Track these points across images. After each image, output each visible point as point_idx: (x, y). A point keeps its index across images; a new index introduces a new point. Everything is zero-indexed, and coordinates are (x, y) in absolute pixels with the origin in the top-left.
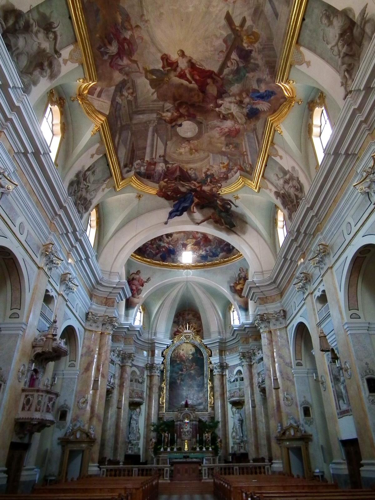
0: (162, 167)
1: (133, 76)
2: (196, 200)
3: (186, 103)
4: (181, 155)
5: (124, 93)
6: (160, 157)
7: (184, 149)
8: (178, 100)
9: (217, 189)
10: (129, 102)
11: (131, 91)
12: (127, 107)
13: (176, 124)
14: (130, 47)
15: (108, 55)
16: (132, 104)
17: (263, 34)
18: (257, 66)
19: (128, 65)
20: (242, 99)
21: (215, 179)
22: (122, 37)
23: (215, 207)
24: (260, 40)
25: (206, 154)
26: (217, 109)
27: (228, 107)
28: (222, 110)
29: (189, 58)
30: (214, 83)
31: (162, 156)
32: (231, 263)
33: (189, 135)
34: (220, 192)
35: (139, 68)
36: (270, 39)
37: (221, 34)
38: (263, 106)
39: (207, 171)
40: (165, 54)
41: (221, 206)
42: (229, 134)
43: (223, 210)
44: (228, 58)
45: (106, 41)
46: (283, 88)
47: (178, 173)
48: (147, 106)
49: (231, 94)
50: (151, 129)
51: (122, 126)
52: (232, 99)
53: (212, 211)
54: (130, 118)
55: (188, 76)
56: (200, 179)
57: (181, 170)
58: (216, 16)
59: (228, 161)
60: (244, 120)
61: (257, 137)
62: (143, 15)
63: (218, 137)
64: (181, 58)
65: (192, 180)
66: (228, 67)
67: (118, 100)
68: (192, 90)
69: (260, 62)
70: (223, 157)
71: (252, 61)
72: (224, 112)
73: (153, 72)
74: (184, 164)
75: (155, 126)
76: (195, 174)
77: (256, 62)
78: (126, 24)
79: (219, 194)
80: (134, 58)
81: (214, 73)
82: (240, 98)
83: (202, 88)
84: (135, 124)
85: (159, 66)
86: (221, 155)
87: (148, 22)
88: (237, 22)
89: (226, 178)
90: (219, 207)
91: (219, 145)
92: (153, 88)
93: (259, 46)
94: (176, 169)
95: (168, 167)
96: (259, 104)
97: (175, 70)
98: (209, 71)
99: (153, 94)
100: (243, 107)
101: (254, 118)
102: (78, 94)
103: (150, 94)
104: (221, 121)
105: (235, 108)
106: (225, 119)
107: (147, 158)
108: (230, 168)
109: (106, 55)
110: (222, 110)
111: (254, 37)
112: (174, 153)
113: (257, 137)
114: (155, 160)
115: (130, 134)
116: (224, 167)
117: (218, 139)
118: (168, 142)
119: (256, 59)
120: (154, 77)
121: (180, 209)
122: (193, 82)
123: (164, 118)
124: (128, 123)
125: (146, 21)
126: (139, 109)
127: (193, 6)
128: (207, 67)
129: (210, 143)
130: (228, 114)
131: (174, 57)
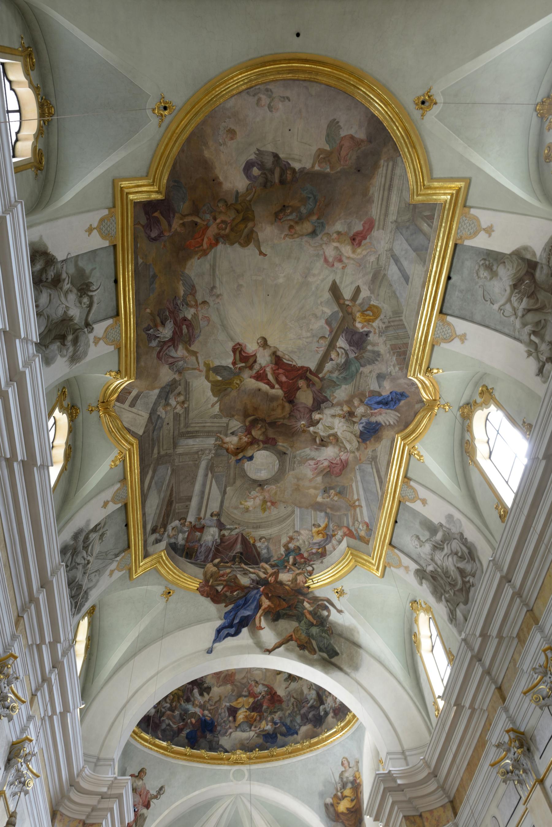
0: (213, 536)
1: (188, 375)
2: (266, 603)
3: (264, 420)
4: (247, 512)
5: (170, 401)
6: (212, 515)
7: (253, 501)
8: (250, 416)
9: (306, 577)
10: (177, 416)
11: (181, 398)
12: (171, 424)
13: (244, 457)
14: (191, 331)
15: (157, 341)
16: (180, 420)
17: (386, 308)
18: (378, 354)
19: (183, 358)
20: (353, 410)
21: (302, 556)
22: (181, 316)
23: (299, 618)
24: (382, 316)
25: (290, 509)
26: (311, 429)
27: (329, 425)
28: (320, 429)
29: (273, 350)
30: (308, 386)
31: (216, 515)
32: (325, 748)
33: (263, 475)
34: (309, 583)
35: (198, 363)
36: (397, 313)
37: (324, 313)
38: (386, 417)
39: (289, 542)
40: (239, 344)
41: (310, 613)
42: (329, 471)
43: (315, 622)
44: (332, 346)
45: (158, 320)
46: (420, 385)
47: (238, 548)
48: (202, 425)
49: (334, 403)
50: (203, 464)
51: (160, 457)
52: (337, 410)
53: (295, 624)
54: (174, 442)
55: (270, 377)
56: (275, 558)
57: (245, 541)
58: (317, 288)
59: (327, 520)
60: (355, 444)
61: (378, 472)
62: (214, 287)
63: (312, 476)
64: (261, 349)
65: (262, 561)
66: (332, 360)
67: (161, 411)
68: (273, 399)
69: (382, 348)
70: (318, 513)
71: (369, 348)
72: (322, 434)
73: (218, 370)
74: (249, 530)
75: (211, 460)
76: (268, 548)
77: (376, 349)
78: (190, 298)
79: (308, 587)
80: (193, 348)
81: (310, 371)
82: (349, 407)
83: (290, 397)
84: (180, 454)
85: (228, 361)
86: (315, 510)
87: (220, 297)
88: (347, 294)
89: (323, 554)
90: (308, 616)
91: (312, 491)
92: (214, 395)
93: (381, 325)
94: (237, 539)
95: (224, 535)
96: (381, 414)
97: (251, 368)
98: (302, 367)
99: (213, 406)
100: (354, 423)
101: (372, 439)
102: (101, 400)
103: (210, 406)
104: (316, 449)
105: (341, 424)
106: (324, 446)
107: (191, 518)
108: (331, 533)
109: (155, 340)
110: (320, 429)
111: (372, 312)
112: (236, 508)
113: (378, 472)
114: (203, 522)
115: (169, 472)
116: (318, 533)
117: (310, 481)
118: (228, 489)
119: (377, 344)
120: (219, 378)
121: (236, 621)
122: (277, 386)
123: (225, 446)
124: (169, 452)
125: (218, 296)
126: (189, 429)
127: (285, 276)
128: (300, 363)
129: (297, 489)
130: (329, 436)
131: (251, 347)
